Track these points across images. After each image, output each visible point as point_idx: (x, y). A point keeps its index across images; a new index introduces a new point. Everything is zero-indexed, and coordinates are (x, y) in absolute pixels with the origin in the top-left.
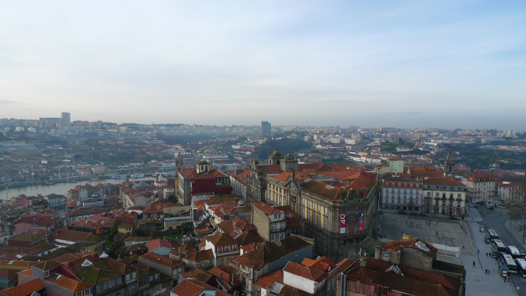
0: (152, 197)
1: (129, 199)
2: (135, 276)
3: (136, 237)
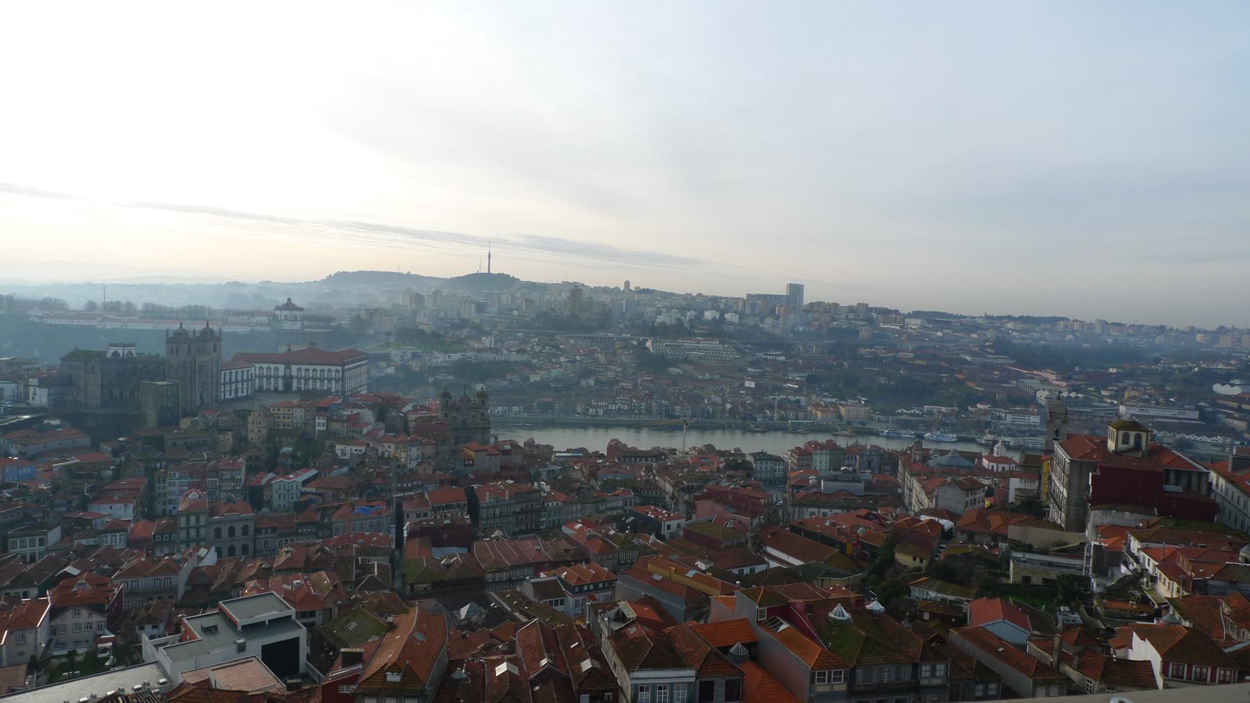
0: (980, 494)
1: (919, 489)
2: (942, 673)
3: (939, 582)
